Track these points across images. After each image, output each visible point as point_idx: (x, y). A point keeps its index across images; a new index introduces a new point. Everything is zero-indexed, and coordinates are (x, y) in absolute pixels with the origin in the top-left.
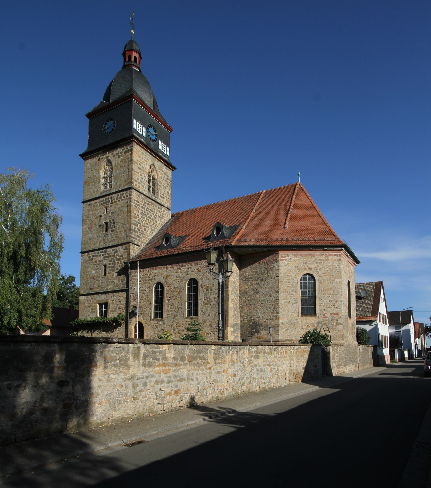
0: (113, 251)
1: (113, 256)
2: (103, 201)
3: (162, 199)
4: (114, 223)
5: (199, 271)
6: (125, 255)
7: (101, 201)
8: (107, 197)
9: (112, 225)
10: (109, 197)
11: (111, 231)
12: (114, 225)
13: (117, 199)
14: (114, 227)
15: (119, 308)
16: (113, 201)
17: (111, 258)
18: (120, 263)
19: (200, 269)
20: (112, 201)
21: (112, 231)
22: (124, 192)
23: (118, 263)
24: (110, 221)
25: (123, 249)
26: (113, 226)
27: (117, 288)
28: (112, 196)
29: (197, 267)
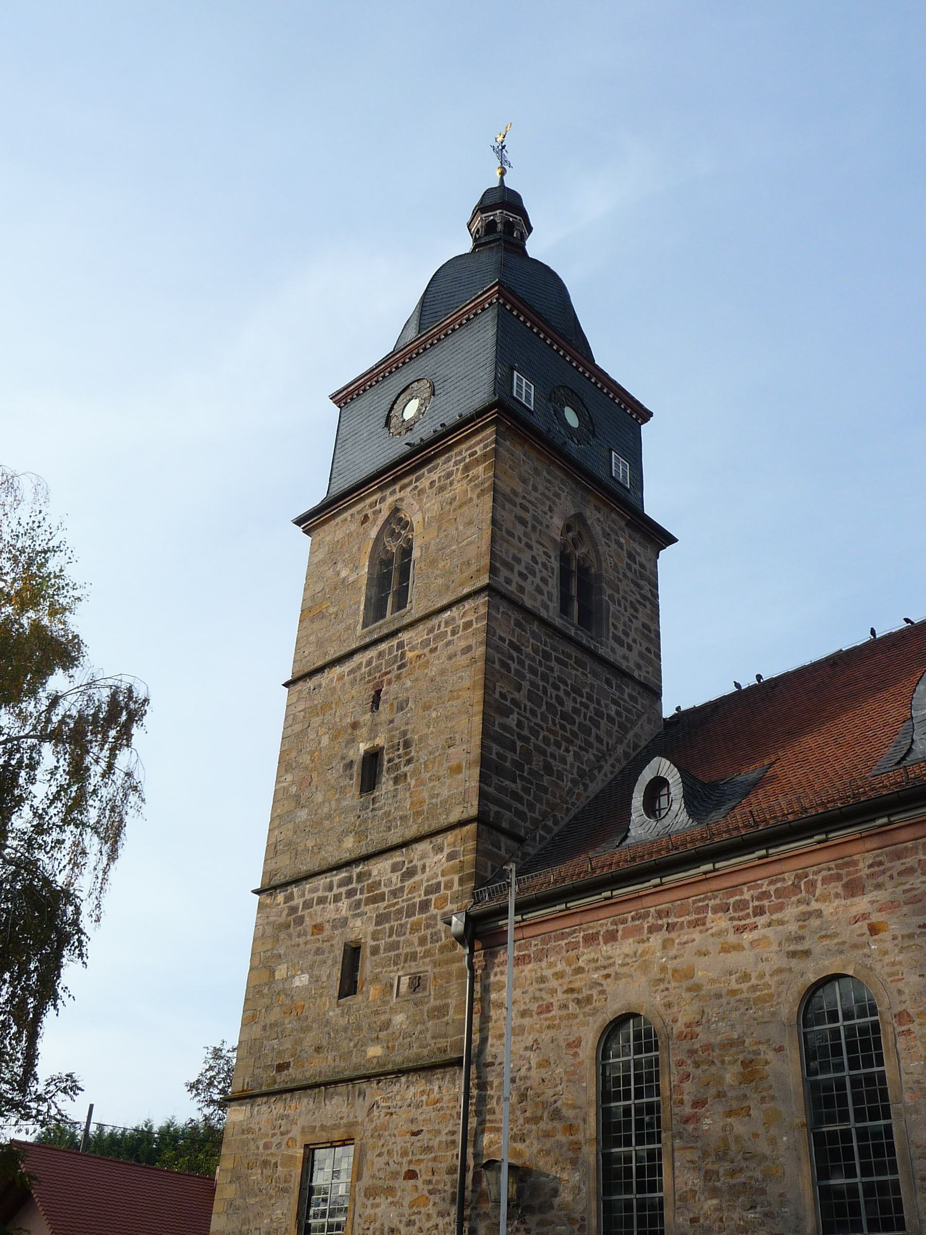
0: (395, 868)
1: (394, 893)
2: (369, 663)
3: (621, 651)
4: (407, 744)
5: (874, 930)
6: (448, 886)
7: (359, 667)
8: (383, 646)
9: (399, 757)
10: (395, 642)
11: (391, 782)
12: (406, 754)
13: (425, 643)
14: (409, 762)
15: (411, 1175)
16: (410, 655)
17: (386, 903)
18: (428, 926)
19: (875, 918)
20: (403, 655)
21: (396, 780)
22: (454, 612)
23: (415, 928)
24: (391, 739)
25: (442, 856)
26: (403, 760)
27: (398, 1058)
28: (404, 636)
29: (862, 904)
